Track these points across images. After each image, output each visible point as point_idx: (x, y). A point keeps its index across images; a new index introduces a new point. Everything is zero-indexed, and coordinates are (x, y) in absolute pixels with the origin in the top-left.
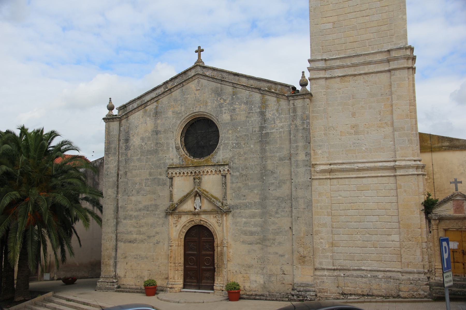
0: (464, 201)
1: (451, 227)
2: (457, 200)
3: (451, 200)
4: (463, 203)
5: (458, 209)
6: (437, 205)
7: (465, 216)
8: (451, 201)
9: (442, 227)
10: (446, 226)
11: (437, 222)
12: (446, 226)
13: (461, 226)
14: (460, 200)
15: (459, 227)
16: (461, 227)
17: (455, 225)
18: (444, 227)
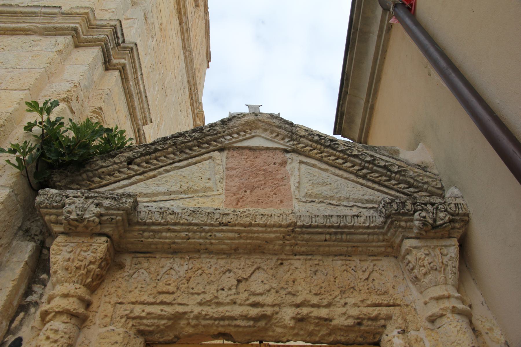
0: (288, 155)
1: (197, 310)
2: (250, 149)
3: (221, 150)
4: (283, 164)
5: (253, 188)
6: (130, 161)
7: (291, 218)
8: (216, 154)
9: (122, 310)
10: (162, 298)
11: (90, 256)
12: (162, 298)
13: (269, 299)
14: (267, 149)
15: (254, 312)
16: (269, 311)
17: (223, 296)
18: (138, 310)
